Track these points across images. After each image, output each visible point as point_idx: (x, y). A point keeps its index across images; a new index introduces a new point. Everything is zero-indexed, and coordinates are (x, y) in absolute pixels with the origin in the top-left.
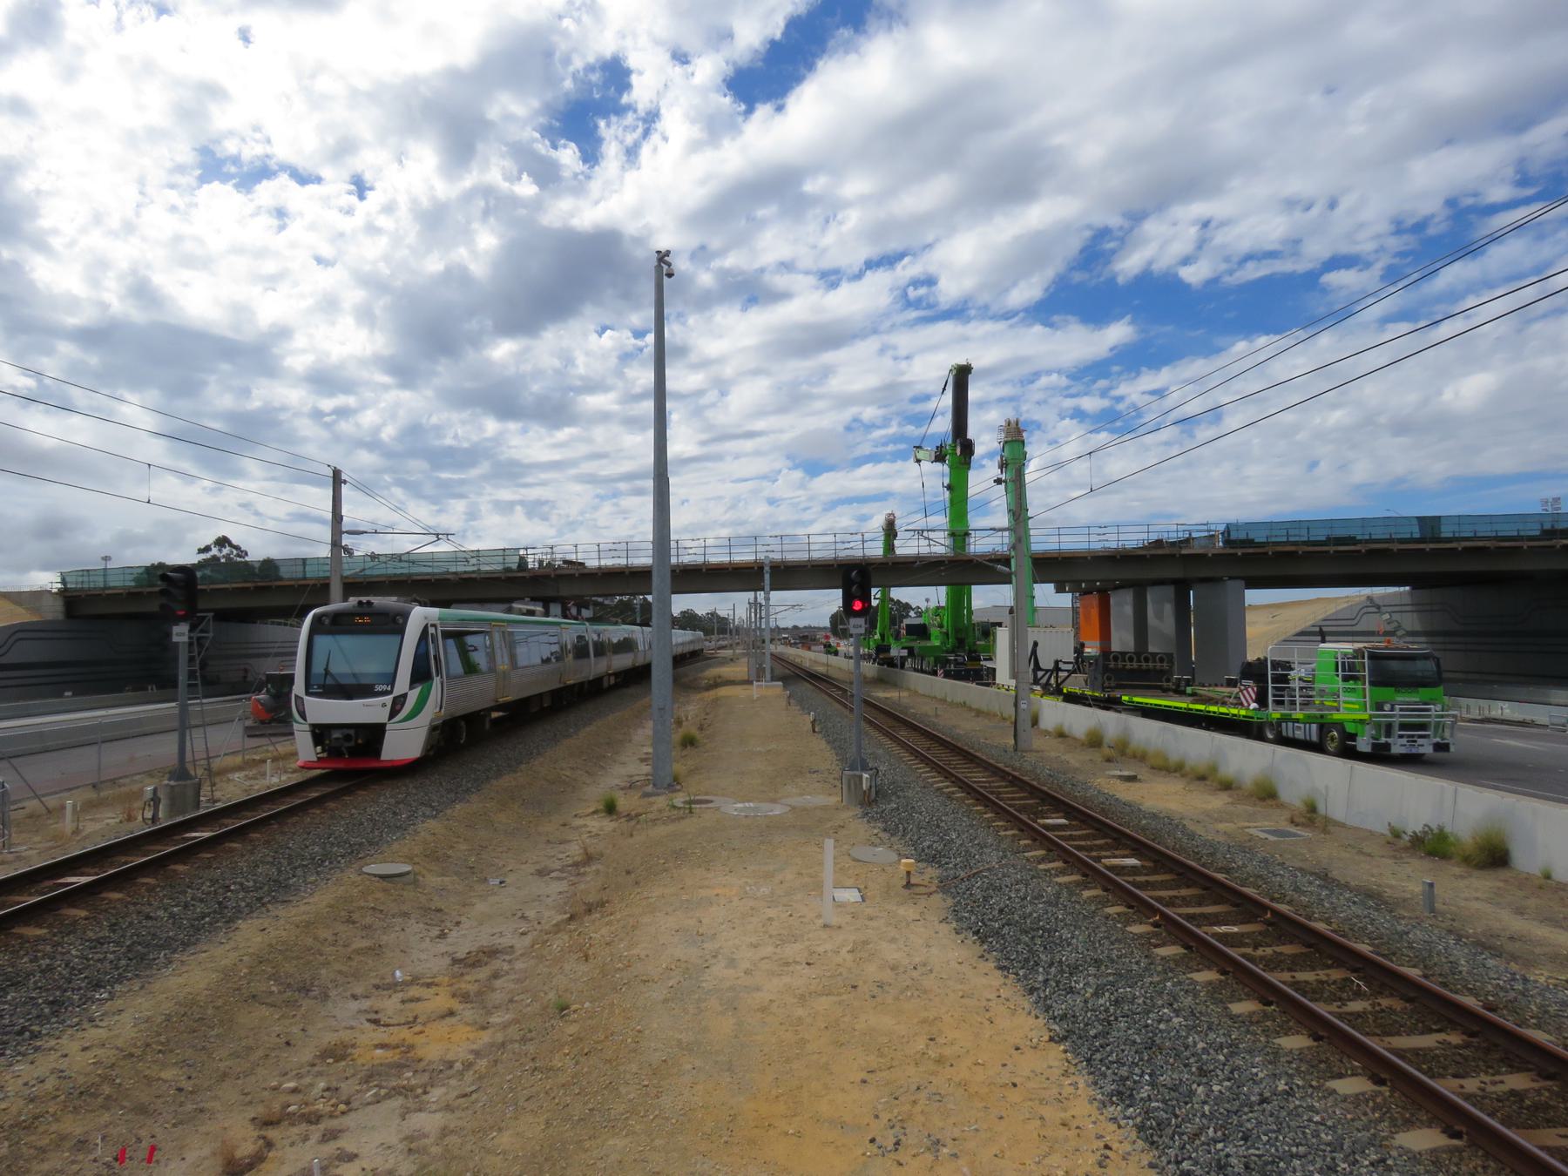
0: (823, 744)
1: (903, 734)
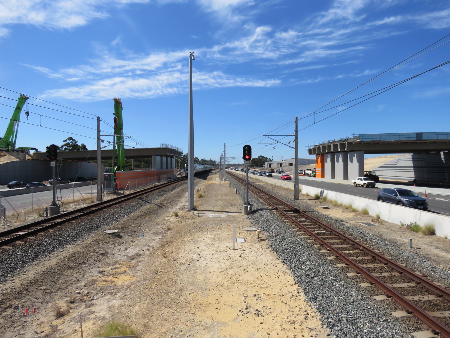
0: (239, 198)
1: (262, 194)
